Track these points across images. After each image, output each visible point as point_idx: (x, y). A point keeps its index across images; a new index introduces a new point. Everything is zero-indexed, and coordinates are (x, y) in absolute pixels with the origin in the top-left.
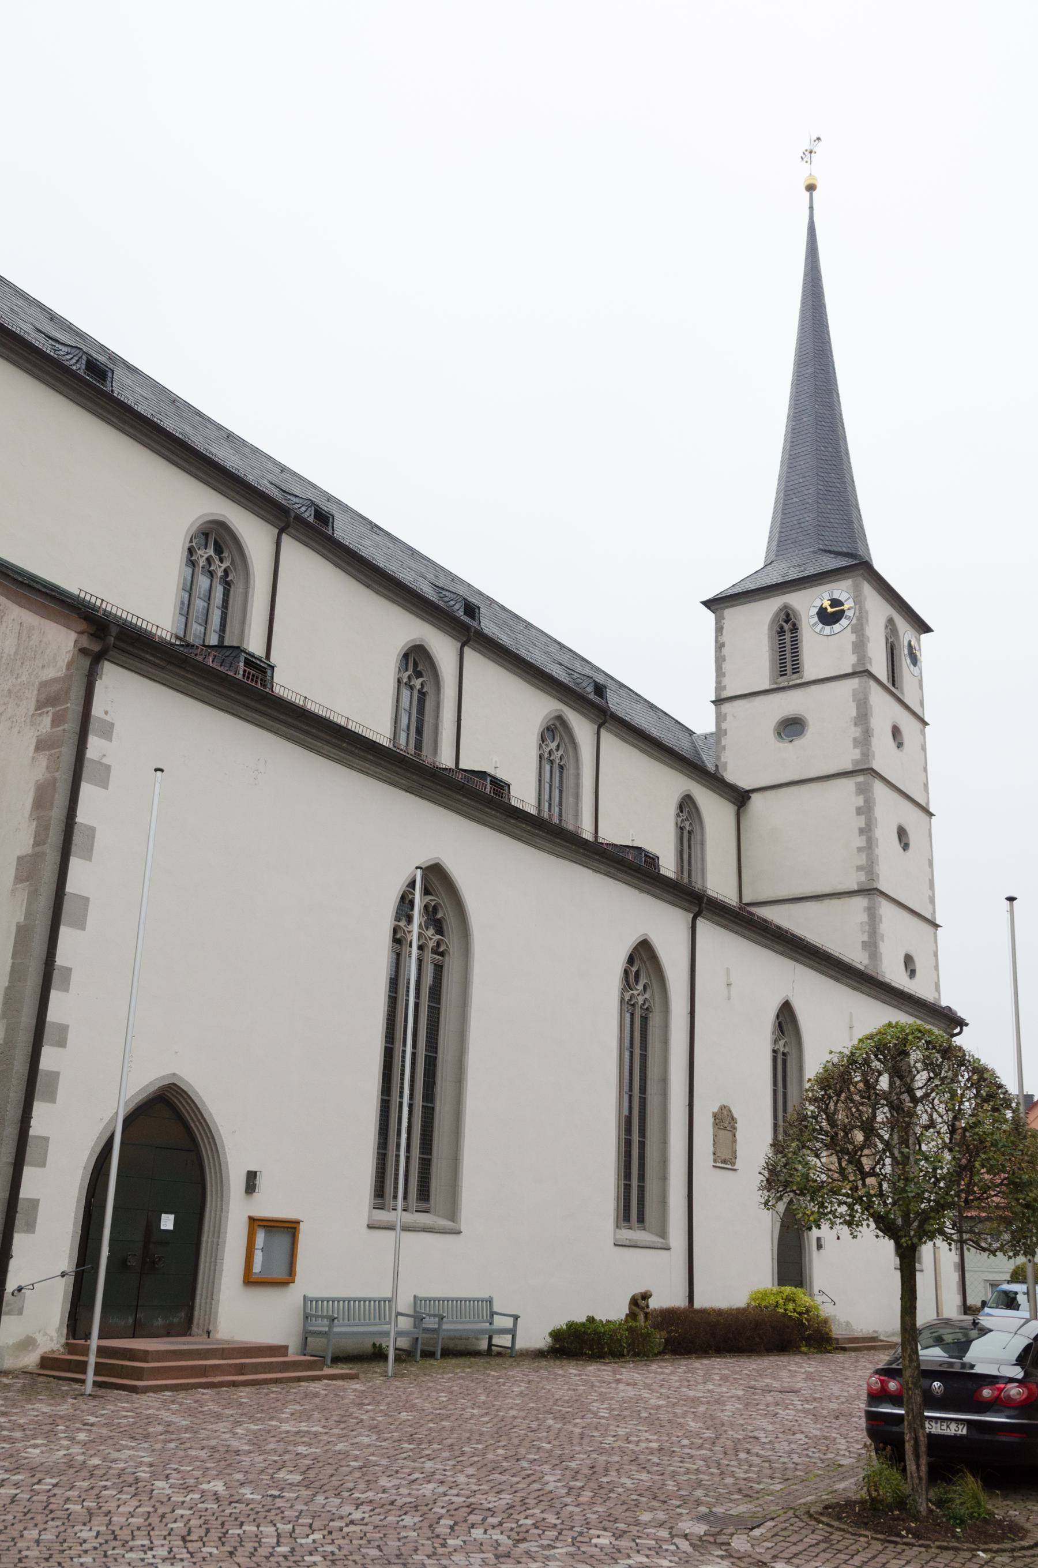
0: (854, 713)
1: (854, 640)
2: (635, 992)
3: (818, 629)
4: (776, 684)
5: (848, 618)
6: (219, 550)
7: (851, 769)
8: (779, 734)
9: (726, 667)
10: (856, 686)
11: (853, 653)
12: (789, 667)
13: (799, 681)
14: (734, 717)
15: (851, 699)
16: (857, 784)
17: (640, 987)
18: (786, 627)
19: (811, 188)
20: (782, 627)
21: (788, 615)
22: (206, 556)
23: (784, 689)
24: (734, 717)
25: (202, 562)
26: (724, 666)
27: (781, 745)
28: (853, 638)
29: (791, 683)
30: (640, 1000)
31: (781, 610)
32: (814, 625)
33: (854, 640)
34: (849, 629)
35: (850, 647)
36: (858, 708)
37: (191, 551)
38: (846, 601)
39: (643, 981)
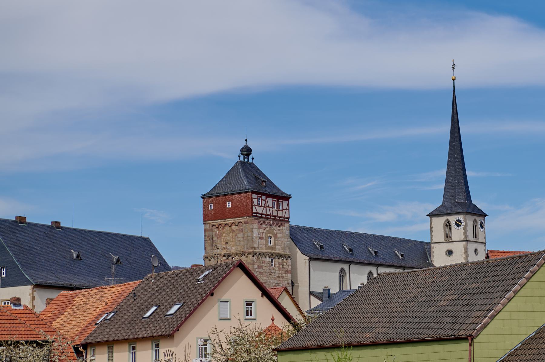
0: (464, 251)
3: (455, 227)
4: (445, 240)
5: (462, 225)
8: (447, 254)
9: (433, 234)
10: (464, 244)
11: (464, 235)
12: (449, 237)
13: (451, 241)
14: (436, 248)
15: (463, 247)
19: (454, 80)
20: (447, 224)
23: (447, 242)
24: (436, 248)
28: (464, 231)
29: (449, 241)
31: (447, 220)
33: (464, 231)
35: (463, 233)
36: (465, 250)
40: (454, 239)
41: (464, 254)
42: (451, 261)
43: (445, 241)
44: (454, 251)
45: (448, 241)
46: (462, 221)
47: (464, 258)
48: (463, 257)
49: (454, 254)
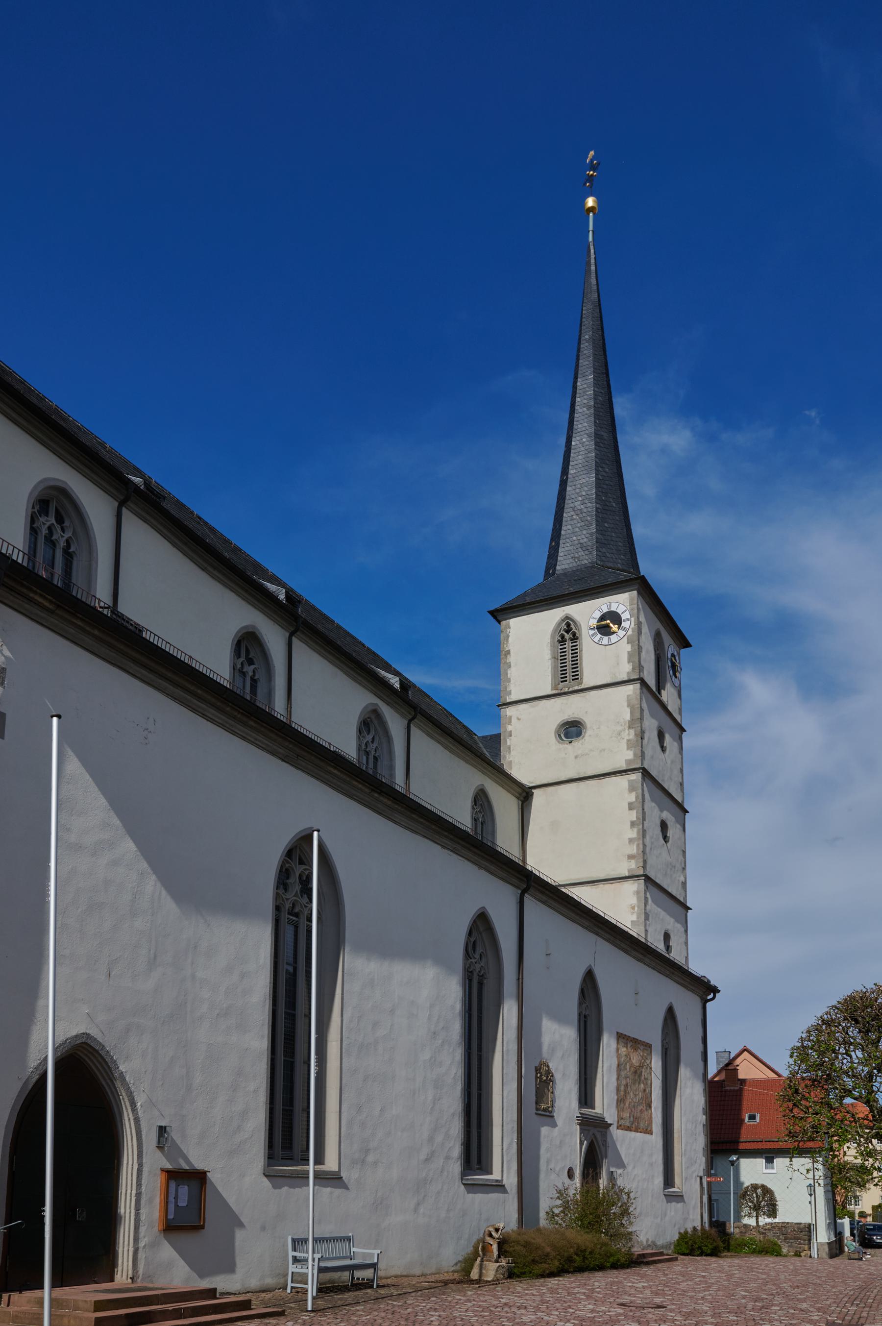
0: (628, 717)
1: (630, 650)
2: (473, 961)
3: (596, 640)
6: (60, 520)
7: (625, 769)
8: (559, 736)
10: (631, 693)
11: (628, 662)
13: (576, 688)
14: (519, 719)
15: (626, 704)
16: (630, 782)
17: (477, 956)
18: (567, 636)
20: (563, 637)
21: (568, 625)
22: (48, 524)
23: (565, 694)
24: (519, 719)
25: (44, 531)
26: (509, 672)
27: (561, 746)
28: (629, 648)
30: (478, 967)
31: (563, 620)
32: (593, 635)
33: (630, 650)
34: (625, 639)
35: (625, 657)
37: (33, 521)
38: (623, 613)
39: (479, 950)
40: (588, 680)
41: (629, 728)
42: (576, 757)
43: (554, 692)
44: (588, 720)
45: (566, 690)
46: (625, 616)
47: (628, 741)
48: (627, 738)
49: (588, 734)
